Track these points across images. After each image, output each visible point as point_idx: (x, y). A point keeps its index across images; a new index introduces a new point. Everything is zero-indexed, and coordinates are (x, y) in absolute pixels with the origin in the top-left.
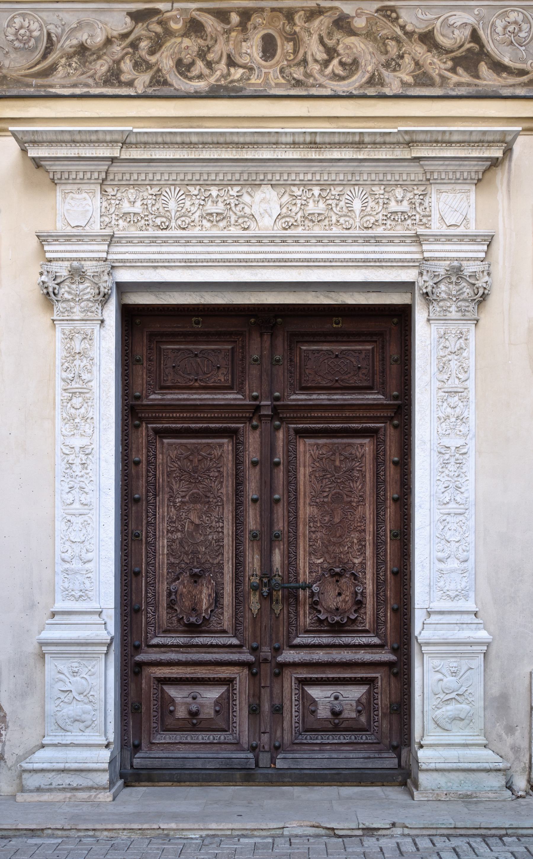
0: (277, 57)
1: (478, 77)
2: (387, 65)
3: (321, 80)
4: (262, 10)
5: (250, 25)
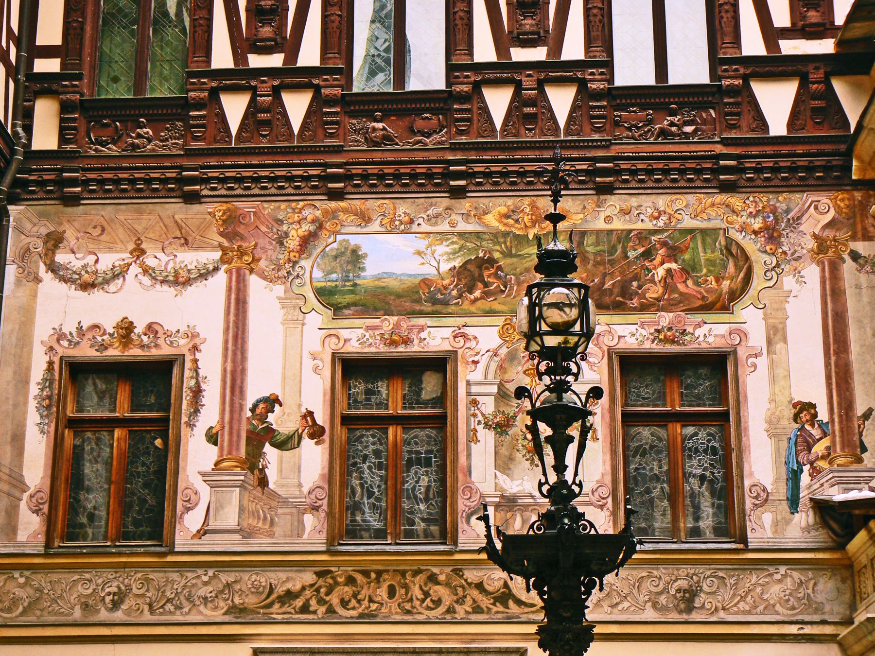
0: (396, 597)
1: (508, 608)
2: (457, 602)
3: (421, 610)
4: (387, 571)
5: (381, 580)
